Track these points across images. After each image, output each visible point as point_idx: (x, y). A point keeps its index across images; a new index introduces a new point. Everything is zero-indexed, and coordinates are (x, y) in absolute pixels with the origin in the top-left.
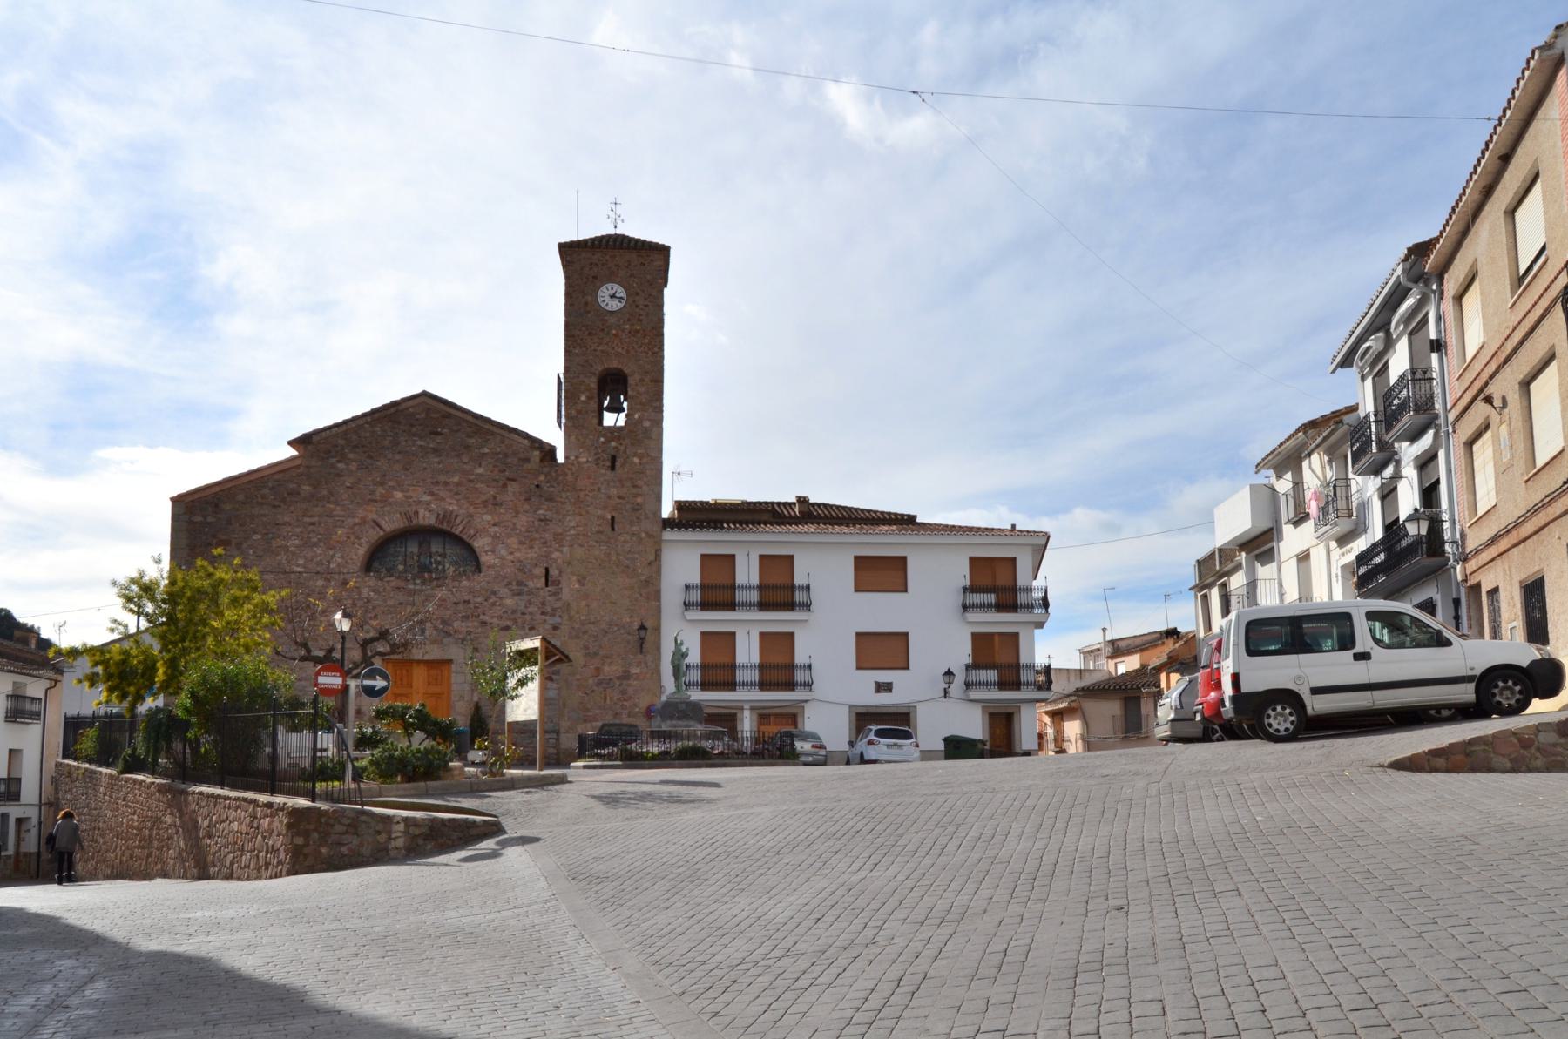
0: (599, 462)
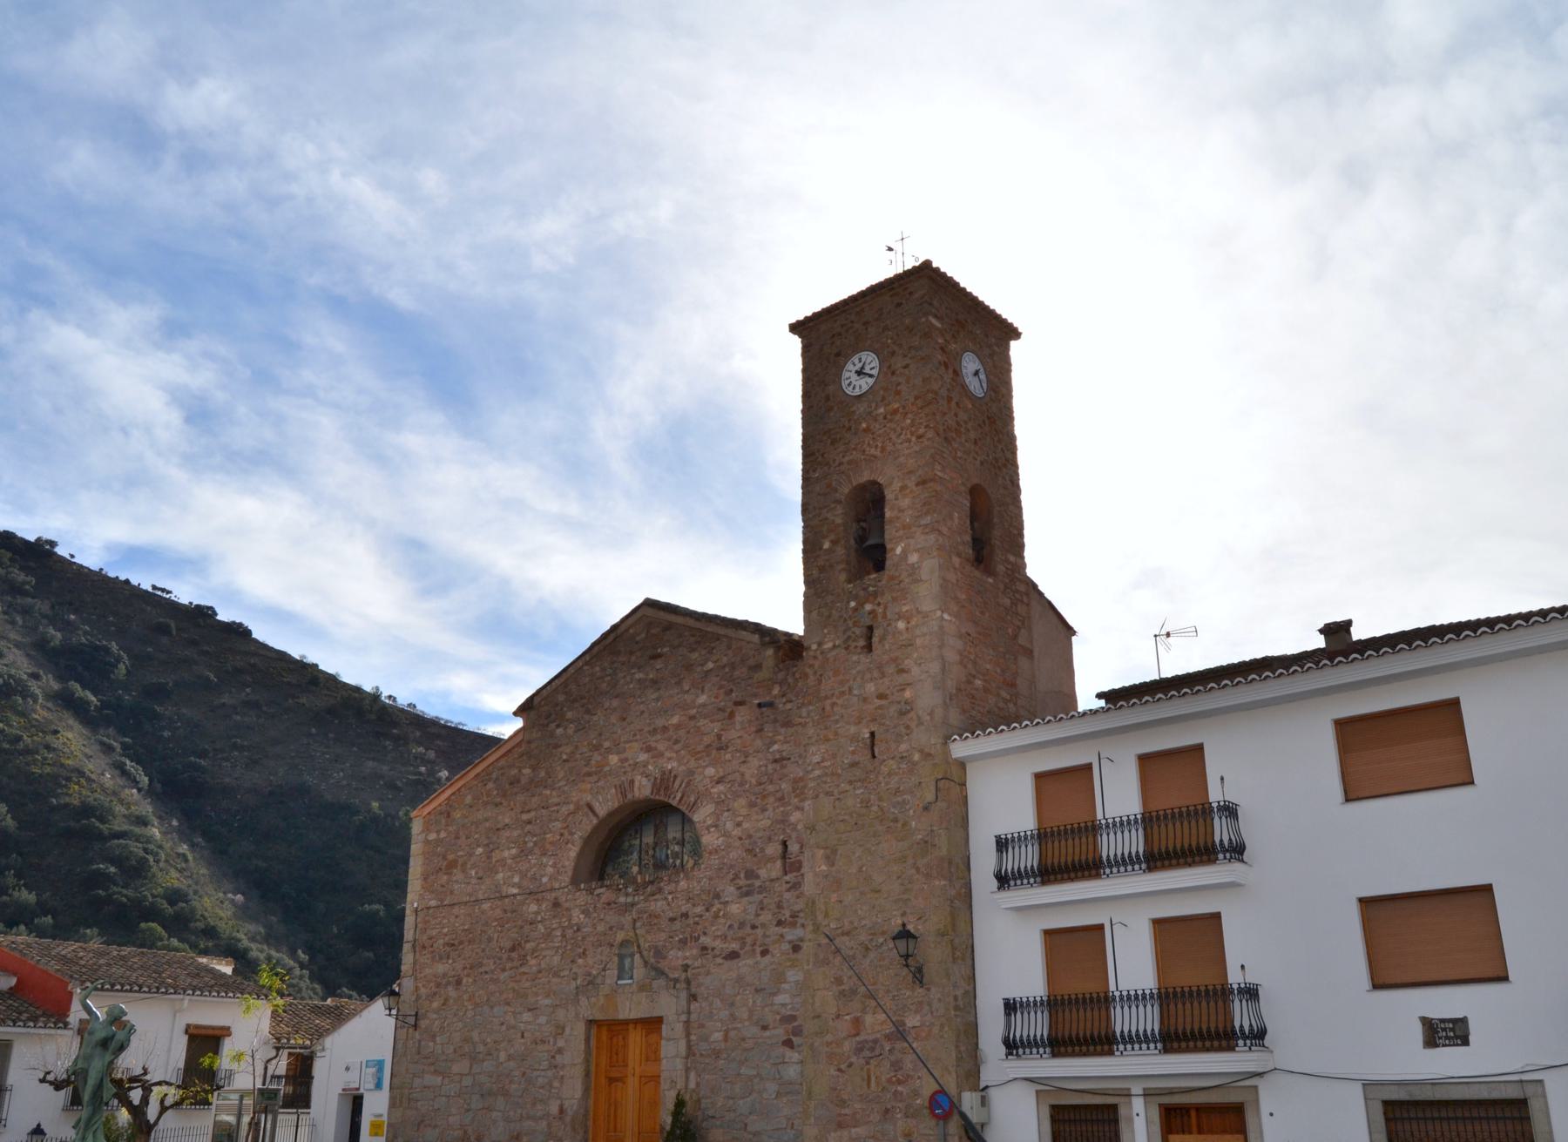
0: (850, 643)
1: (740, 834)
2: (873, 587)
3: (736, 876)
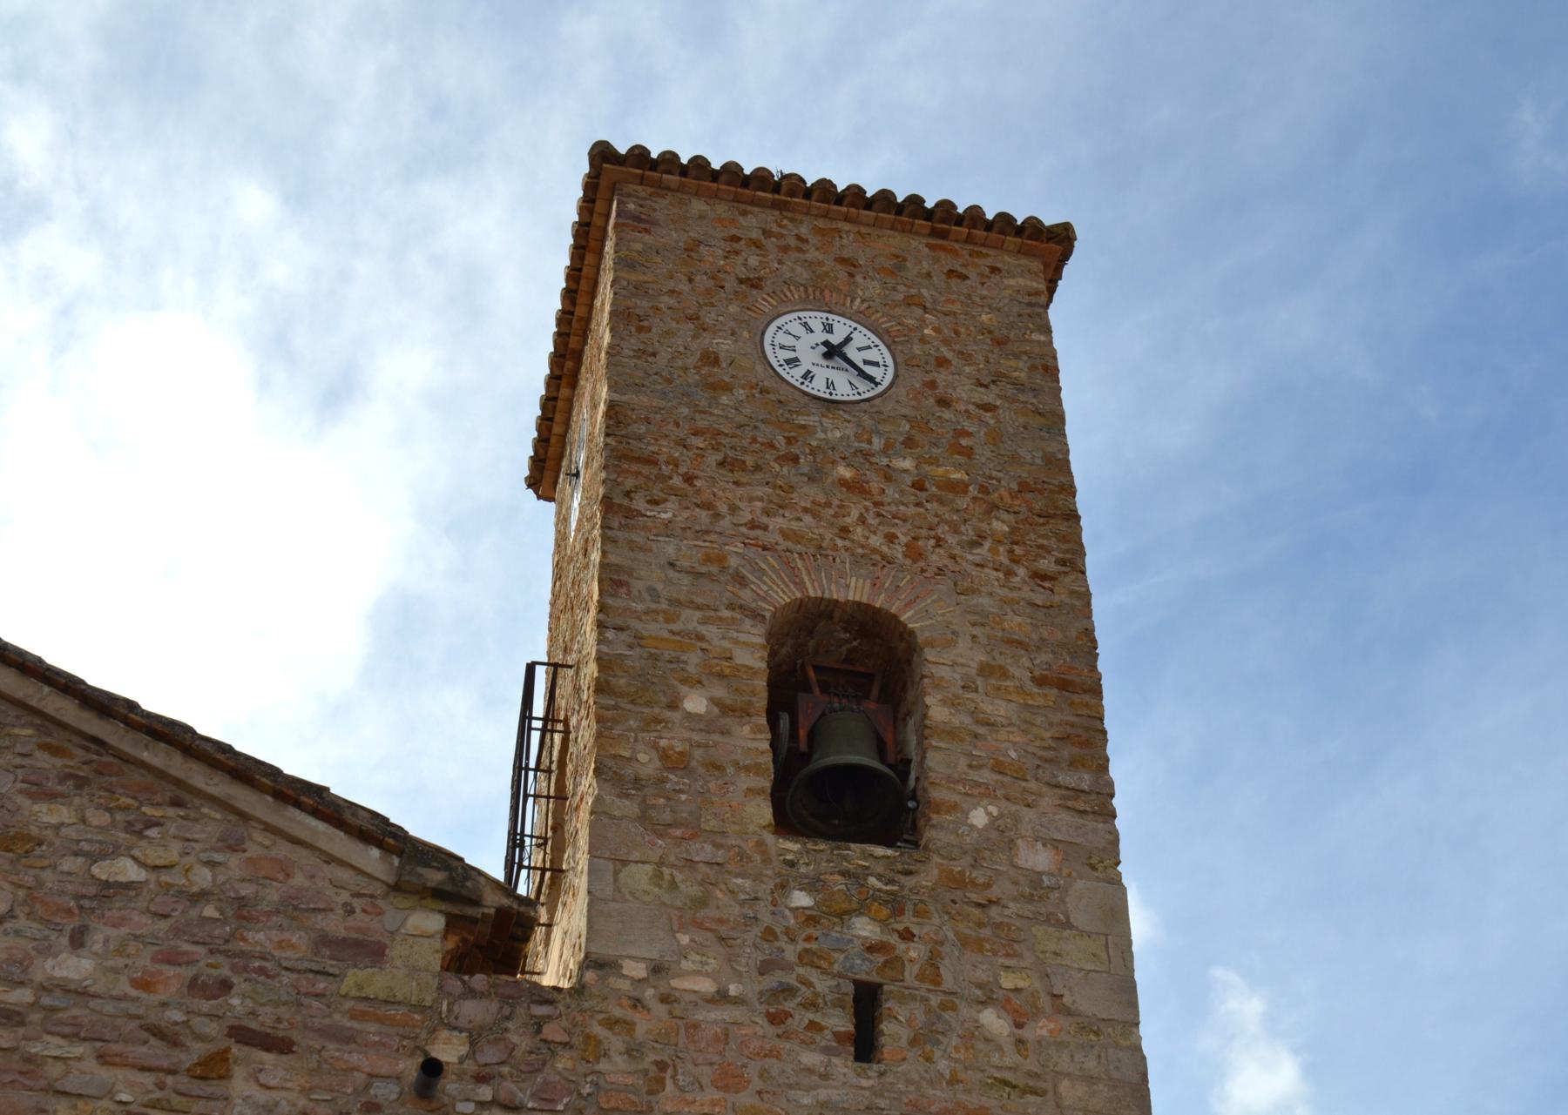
0: (789, 1005)
2: (880, 877)
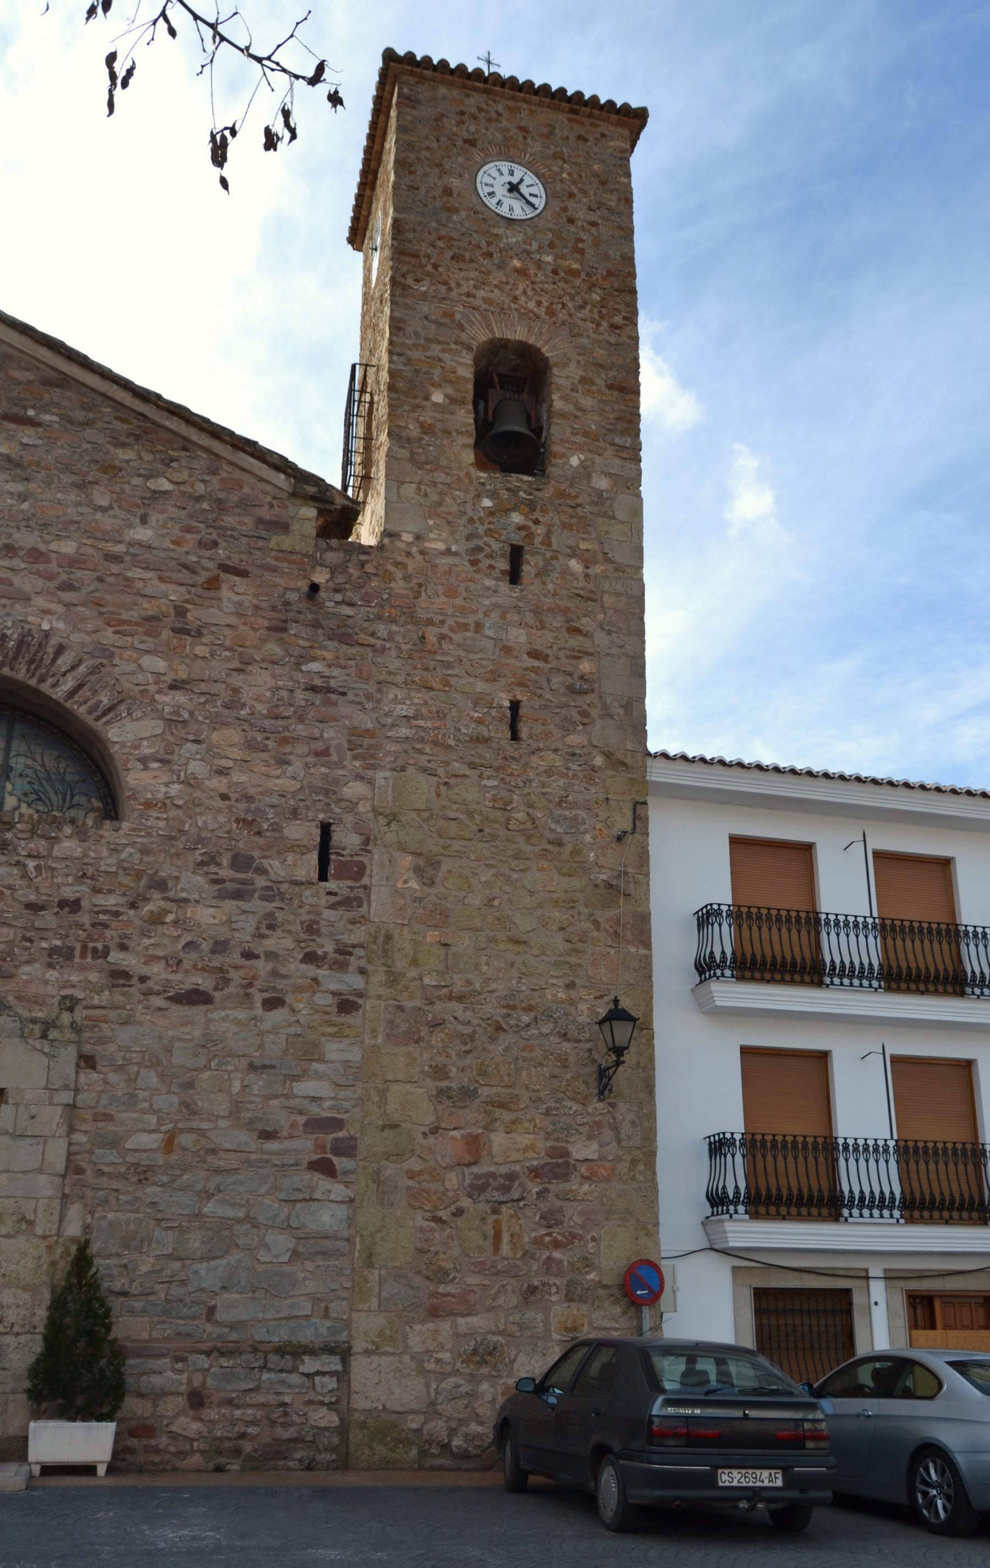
0: (480, 556)
1: (223, 789)
2: (525, 492)
3: (211, 860)
